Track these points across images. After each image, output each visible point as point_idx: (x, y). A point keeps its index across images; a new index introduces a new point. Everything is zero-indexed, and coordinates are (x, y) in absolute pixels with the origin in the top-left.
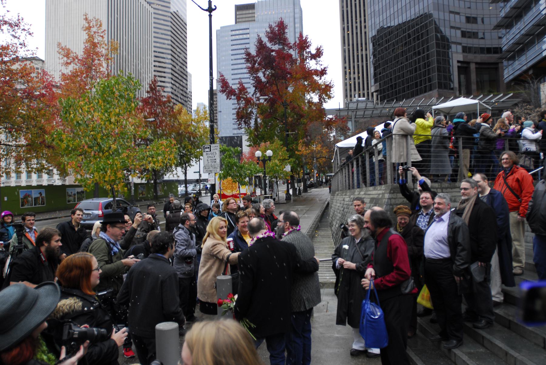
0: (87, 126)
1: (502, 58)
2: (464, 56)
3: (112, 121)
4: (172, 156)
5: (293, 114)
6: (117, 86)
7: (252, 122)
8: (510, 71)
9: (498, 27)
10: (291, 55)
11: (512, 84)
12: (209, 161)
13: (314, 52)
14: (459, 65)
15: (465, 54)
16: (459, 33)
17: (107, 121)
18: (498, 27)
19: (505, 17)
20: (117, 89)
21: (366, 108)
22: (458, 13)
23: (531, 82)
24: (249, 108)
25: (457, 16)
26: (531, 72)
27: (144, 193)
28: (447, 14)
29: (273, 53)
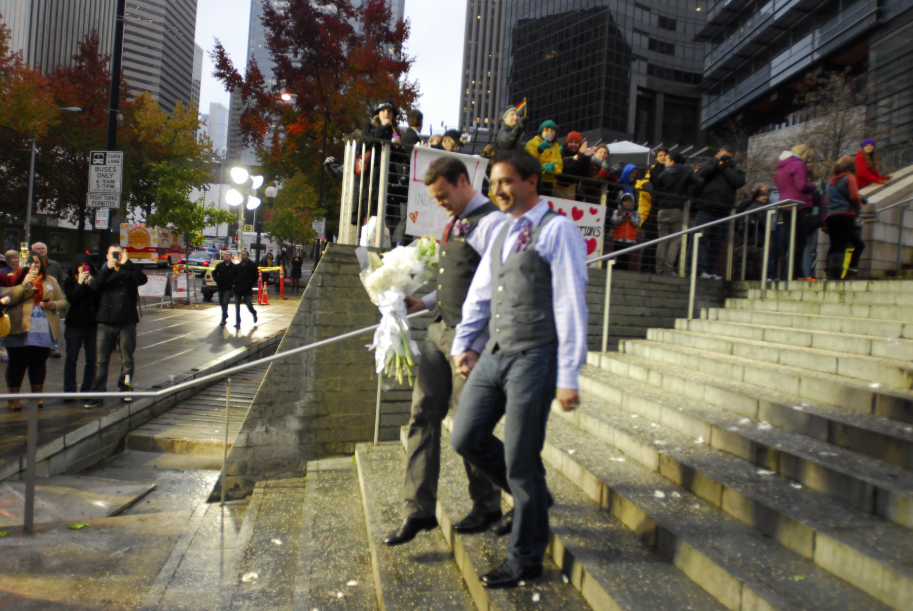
7: (268, 137)
8: (711, 112)
10: (350, 29)
11: (712, 133)
12: (101, 184)
13: (393, 28)
14: (640, 93)
16: (645, 41)
18: (702, 37)
19: (714, 23)
22: (648, 9)
23: (734, 131)
24: (264, 112)
25: (646, 14)
26: (739, 118)
27: (62, 246)
28: (630, 8)
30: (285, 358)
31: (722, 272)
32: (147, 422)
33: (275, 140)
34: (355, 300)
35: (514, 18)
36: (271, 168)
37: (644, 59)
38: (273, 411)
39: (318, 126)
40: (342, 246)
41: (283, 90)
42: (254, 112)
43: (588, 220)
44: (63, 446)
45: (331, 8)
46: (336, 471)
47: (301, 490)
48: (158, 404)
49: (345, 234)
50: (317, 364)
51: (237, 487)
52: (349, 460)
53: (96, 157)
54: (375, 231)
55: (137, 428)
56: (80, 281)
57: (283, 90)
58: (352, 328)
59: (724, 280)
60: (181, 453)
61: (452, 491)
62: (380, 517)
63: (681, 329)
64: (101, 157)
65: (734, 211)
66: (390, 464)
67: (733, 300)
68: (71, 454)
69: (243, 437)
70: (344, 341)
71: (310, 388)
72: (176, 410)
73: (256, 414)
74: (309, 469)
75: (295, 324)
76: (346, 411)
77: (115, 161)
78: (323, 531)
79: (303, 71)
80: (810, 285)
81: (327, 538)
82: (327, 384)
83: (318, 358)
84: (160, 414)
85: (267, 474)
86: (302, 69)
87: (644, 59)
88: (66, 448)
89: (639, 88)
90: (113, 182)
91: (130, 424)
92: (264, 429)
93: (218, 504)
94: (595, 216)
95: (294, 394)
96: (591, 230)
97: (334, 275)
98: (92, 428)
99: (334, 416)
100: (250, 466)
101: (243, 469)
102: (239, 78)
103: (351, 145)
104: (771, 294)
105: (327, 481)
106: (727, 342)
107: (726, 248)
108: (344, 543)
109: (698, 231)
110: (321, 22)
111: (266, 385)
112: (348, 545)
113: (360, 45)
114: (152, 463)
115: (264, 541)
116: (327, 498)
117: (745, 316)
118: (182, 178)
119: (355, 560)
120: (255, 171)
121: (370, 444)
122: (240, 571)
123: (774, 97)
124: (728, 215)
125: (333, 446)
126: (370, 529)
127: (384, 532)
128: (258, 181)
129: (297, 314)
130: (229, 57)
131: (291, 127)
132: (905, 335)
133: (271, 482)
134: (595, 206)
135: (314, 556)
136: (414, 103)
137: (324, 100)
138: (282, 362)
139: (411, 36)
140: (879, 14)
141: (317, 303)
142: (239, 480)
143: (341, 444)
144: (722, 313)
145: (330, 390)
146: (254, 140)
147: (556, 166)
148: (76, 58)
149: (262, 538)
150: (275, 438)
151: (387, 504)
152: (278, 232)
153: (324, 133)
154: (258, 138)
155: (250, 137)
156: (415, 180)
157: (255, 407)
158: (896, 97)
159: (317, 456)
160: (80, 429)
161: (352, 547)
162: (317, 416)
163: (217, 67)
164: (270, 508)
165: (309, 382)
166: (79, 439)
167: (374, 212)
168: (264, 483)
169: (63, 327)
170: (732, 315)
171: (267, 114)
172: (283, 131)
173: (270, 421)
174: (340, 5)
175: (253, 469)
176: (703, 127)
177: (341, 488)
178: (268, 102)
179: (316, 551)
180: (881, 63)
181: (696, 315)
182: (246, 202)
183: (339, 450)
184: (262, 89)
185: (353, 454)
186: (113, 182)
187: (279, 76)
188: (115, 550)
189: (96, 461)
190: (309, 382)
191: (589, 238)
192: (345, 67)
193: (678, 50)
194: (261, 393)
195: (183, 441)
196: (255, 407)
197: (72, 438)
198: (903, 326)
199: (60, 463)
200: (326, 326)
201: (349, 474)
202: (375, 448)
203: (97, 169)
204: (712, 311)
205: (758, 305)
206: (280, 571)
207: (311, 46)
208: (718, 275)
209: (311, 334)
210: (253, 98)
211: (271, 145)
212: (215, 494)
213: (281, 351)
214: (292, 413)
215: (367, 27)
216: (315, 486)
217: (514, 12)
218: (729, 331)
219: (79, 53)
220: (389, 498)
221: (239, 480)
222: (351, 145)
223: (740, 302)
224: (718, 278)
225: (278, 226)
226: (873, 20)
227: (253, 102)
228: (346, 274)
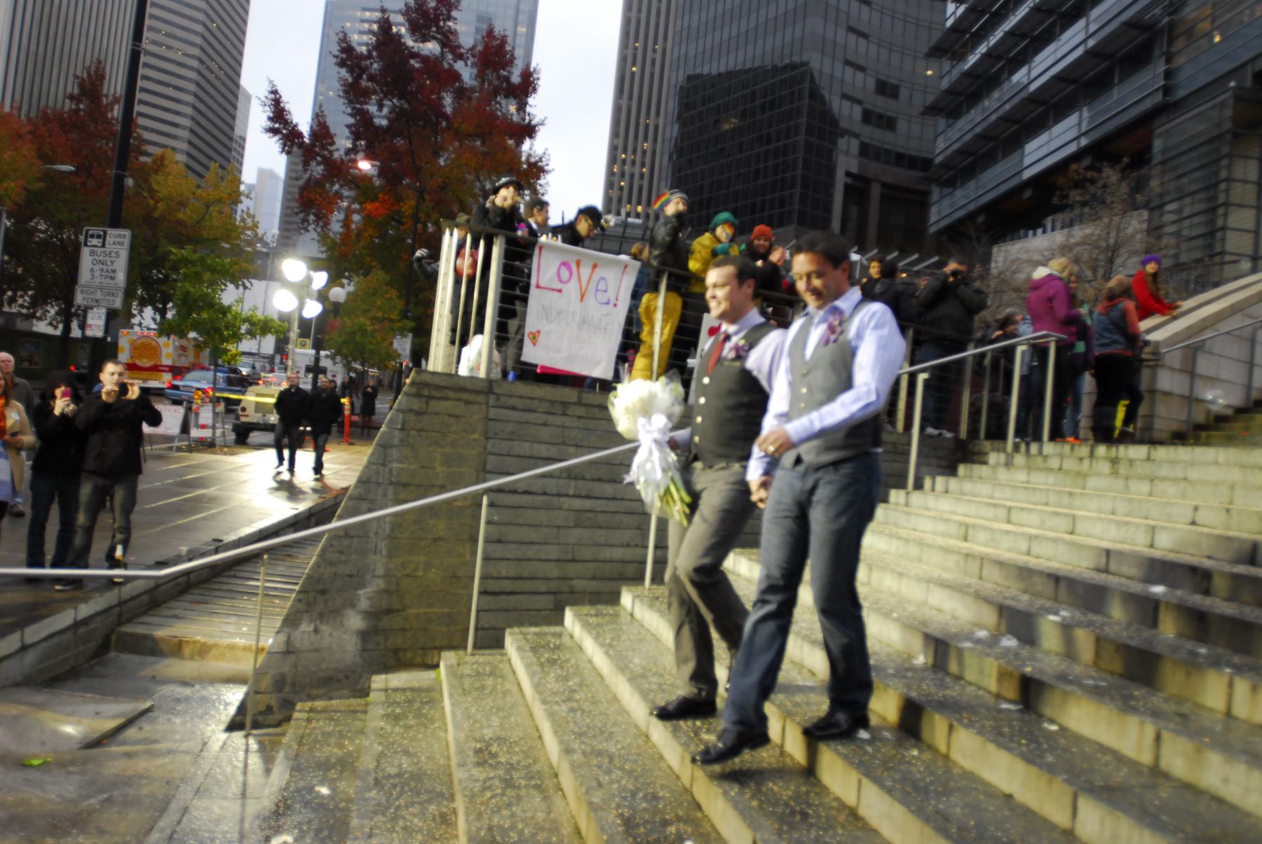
8: (944, 209)
9: (933, 110)
10: (457, 76)
11: (944, 238)
12: (97, 273)
13: (516, 79)
14: (849, 181)
16: (857, 111)
18: (933, 110)
19: (949, 92)
21: (623, 237)
24: (333, 184)
25: (860, 75)
26: (981, 219)
27: (36, 358)
29: (415, 63)
30: (346, 529)
31: (954, 427)
32: (145, 613)
33: (346, 223)
34: (447, 450)
35: (681, 71)
36: (338, 262)
37: (857, 136)
38: (326, 602)
39: (408, 207)
40: (434, 373)
41: (361, 155)
44: (19, 645)
45: (432, 47)
46: (412, 690)
47: (361, 716)
48: (163, 588)
49: (437, 360)
50: (391, 538)
51: (269, 709)
52: (431, 674)
53: (92, 236)
54: (480, 354)
55: (129, 621)
56: (57, 412)
57: (361, 155)
58: (443, 489)
59: (956, 438)
60: (191, 658)
61: (575, 723)
62: (471, 758)
63: (897, 504)
64: (99, 237)
65: (971, 345)
66: (489, 682)
67: (969, 466)
68: (30, 657)
69: (282, 638)
71: (380, 571)
72: (188, 597)
73: (301, 606)
74: (374, 686)
75: (363, 481)
76: (430, 605)
77: (121, 244)
78: (390, 776)
79: (389, 131)
80: (1072, 449)
81: (395, 786)
82: (404, 566)
83: (392, 530)
84: (164, 602)
85: (314, 692)
86: (389, 128)
87: (857, 136)
88: (24, 648)
89: (848, 174)
90: (114, 271)
91: (120, 615)
92: (312, 628)
93: (242, 733)
95: (356, 579)
97: (419, 413)
98: (64, 619)
99: (413, 611)
100: (289, 679)
101: (279, 683)
102: (300, 135)
103: (451, 235)
104: (1019, 459)
105: (399, 704)
106: (960, 524)
107: (960, 394)
108: (419, 794)
109: (923, 370)
110: (417, 65)
111: (317, 565)
112: (424, 797)
113: (470, 99)
114: (146, 672)
115: (304, 788)
116: (397, 730)
117: (984, 489)
118: (213, 270)
119: (434, 819)
120: (316, 265)
121: (461, 652)
122: (268, 832)
123: (1028, 194)
124: (963, 349)
125: (409, 655)
126: (458, 774)
127: (477, 780)
128: (320, 279)
129: (366, 467)
130: (287, 107)
131: (368, 206)
132: (1199, 520)
133: (319, 704)
135: (375, 813)
136: (541, 181)
137: (416, 172)
138: (342, 533)
139: (540, 90)
140: (1167, 90)
141: (394, 453)
142: (273, 700)
143: (420, 652)
144: (953, 483)
145: (408, 576)
146: (316, 222)
148: (71, 97)
149: (301, 784)
151: (482, 740)
152: (345, 351)
153: (416, 218)
154: (323, 219)
155: (312, 218)
156: (538, 287)
157: (301, 596)
158: (1187, 200)
159: (386, 668)
160: (46, 622)
161: (429, 801)
162: (388, 612)
163: (270, 119)
164: (316, 741)
165: (379, 564)
166: (44, 634)
167: (480, 329)
168: (309, 704)
169: (28, 474)
170: (967, 486)
171: (336, 187)
172: (358, 212)
173: (322, 617)
175: (294, 684)
176: (932, 230)
177: (419, 715)
178: (339, 170)
179: (379, 804)
180: (1170, 154)
181: (919, 486)
183: (419, 660)
184: (331, 152)
185: (436, 666)
186: (114, 271)
187: (356, 136)
188: (88, 797)
189: (68, 667)
190: (379, 564)
192: (449, 127)
193: (902, 126)
194: (310, 577)
195: (195, 642)
196: (301, 596)
197: (34, 633)
198: (1196, 508)
199: (14, 669)
200: (405, 485)
201: (430, 696)
202: (469, 659)
203: (92, 253)
204: (940, 480)
205: (1003, 474)
206: (326, 833)
208: (949, 430)
209: (385, 495)
210: (318, 164)
211: (341, 230)
212: (238, 718)
213: (341, 518)
214: (353, 606)
215: (480, 76)
216: (381, 711)
217: (682, 64)
218: (962, 508)
219: (76, 91)
220: (486, 731)
221: (273, 700)
222: (451, 235)
223: (978, 470)
224: (949, 435)
225: (345, 342)
226: (1159, 98)
227: (318, 170)
228: (437, 414)
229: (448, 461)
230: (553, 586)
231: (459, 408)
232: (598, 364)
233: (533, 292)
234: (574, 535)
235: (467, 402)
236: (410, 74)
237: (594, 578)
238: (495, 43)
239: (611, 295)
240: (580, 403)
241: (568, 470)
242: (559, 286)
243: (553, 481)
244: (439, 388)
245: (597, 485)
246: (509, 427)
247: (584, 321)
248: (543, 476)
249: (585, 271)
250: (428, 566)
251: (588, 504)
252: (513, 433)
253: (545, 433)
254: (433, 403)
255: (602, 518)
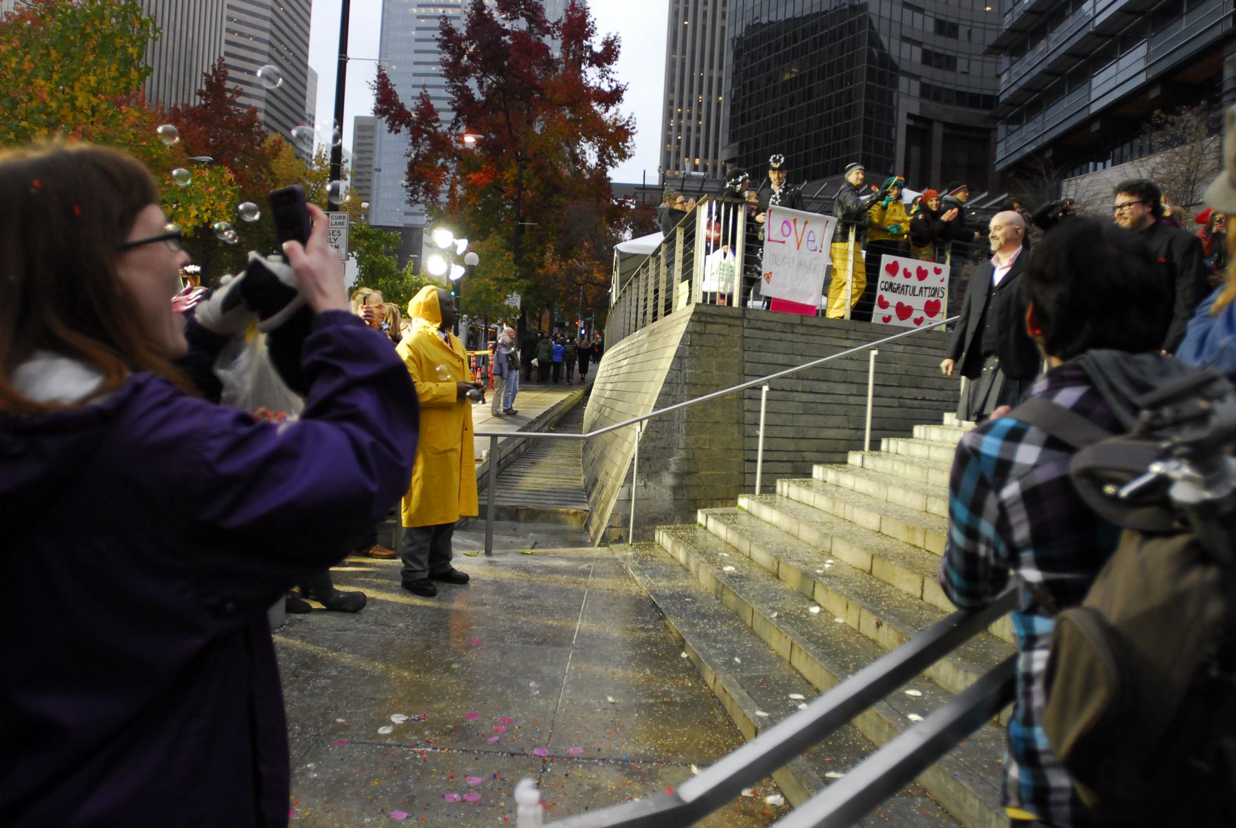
0: (14, 103)
1: (996, 118)
2: (922, 105)
3: (78, 103)
4: (224, 204)
5: (536, 182)
6: (97, 22)
8: (1009, 147)
9: (996, 49)
10: (546, 49)
11: (1011, 175)
13: (598, 48)
14: (911, 123)
15: (926, 102)
16: (917, 53)
17: (66, 101)
18: (996, 49)
19: (1012, 30)
20: (96, 31)
22: (921, 10)
24: (438, 158)
25: (918, 16)
26: (1048, 154)
28: (897, 9)
35: (739, 25)
36: (474, 229)
37: (917, 77)
39: (510, 174)
42: (426, 158)
43: (932, 280)
45: (522, 24)
57: (463, 129)
58: (718, 388)
70: (711, 400)
71: (682, 445)
76: (714, 469)
77: (342, 224)
86: (486, 103)
87: (917, 77)
89: (910, 116)
94: (939, 276)
95: (668, 450)
96: (936, 290)
97: (701, 334)
99: (704, 473)
110: (510, 42)
113: (557, 70)
123: (1096, 127)
128: (463, 244)
130: (397, 89)
134: (939, 266)
139: (620, 56)
147: (902, 225)
148: (201, 93)
150: (652, 492)
152: (472, 309)
154: (432, 191)
162: (689, 473)
171: (441, 161)
174: (530, 20)
176: (999, 167)
178: (441, 144)
182: (448, 273)
184: (435, 128)
187: (459, 111)
191: (933, 299)
192: (541, 99)
200: (695, 385)
207: (500, 72)
210: (424, 140)
214: (667, 469)
215: (565, 46)
219: (204, 88)
225: (471, 302)
227: (425, 148)
229: (720, 368)
230: (791, 456)
231: (726, 330)
232: (810, 295)
233: (766, 243)
234: (804, 420)
235: (730, 325)
236: (504, 51)
237: (818, 451)
238: (577, 15)
239: (818, 244)
240: (802, 324)
241: (797, 373)
242: (783, 239)
243: (787, 381)
244: (712, 315)
245: (816, 383)
246: (758, 342)
247: (800, 264)
248: (782, 377)
249: (800, 227)
250: (711, 441)
251: (811, 397)
252: (760, 347)
253: (781, 346)
254: (709, 326)
255: (821, 408)
